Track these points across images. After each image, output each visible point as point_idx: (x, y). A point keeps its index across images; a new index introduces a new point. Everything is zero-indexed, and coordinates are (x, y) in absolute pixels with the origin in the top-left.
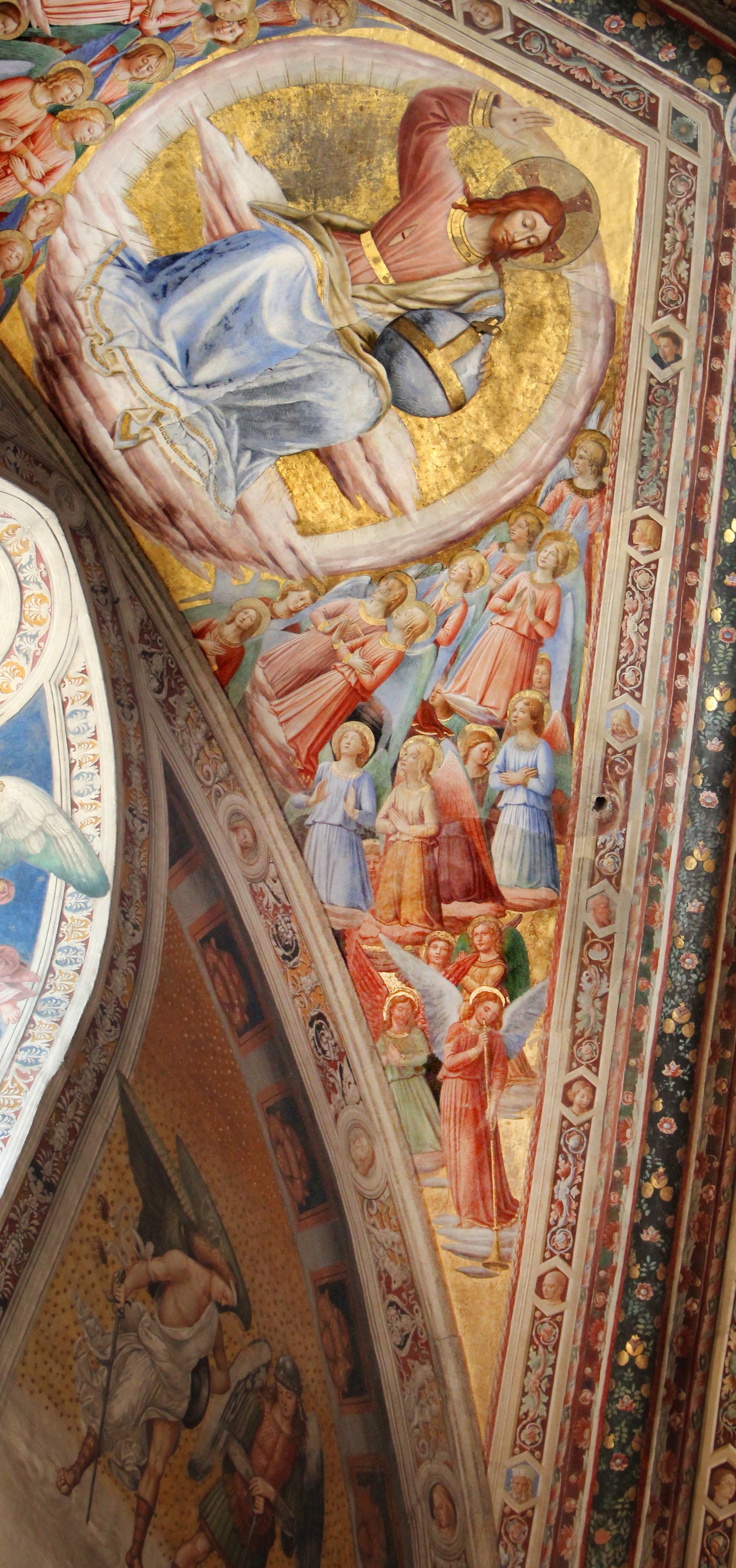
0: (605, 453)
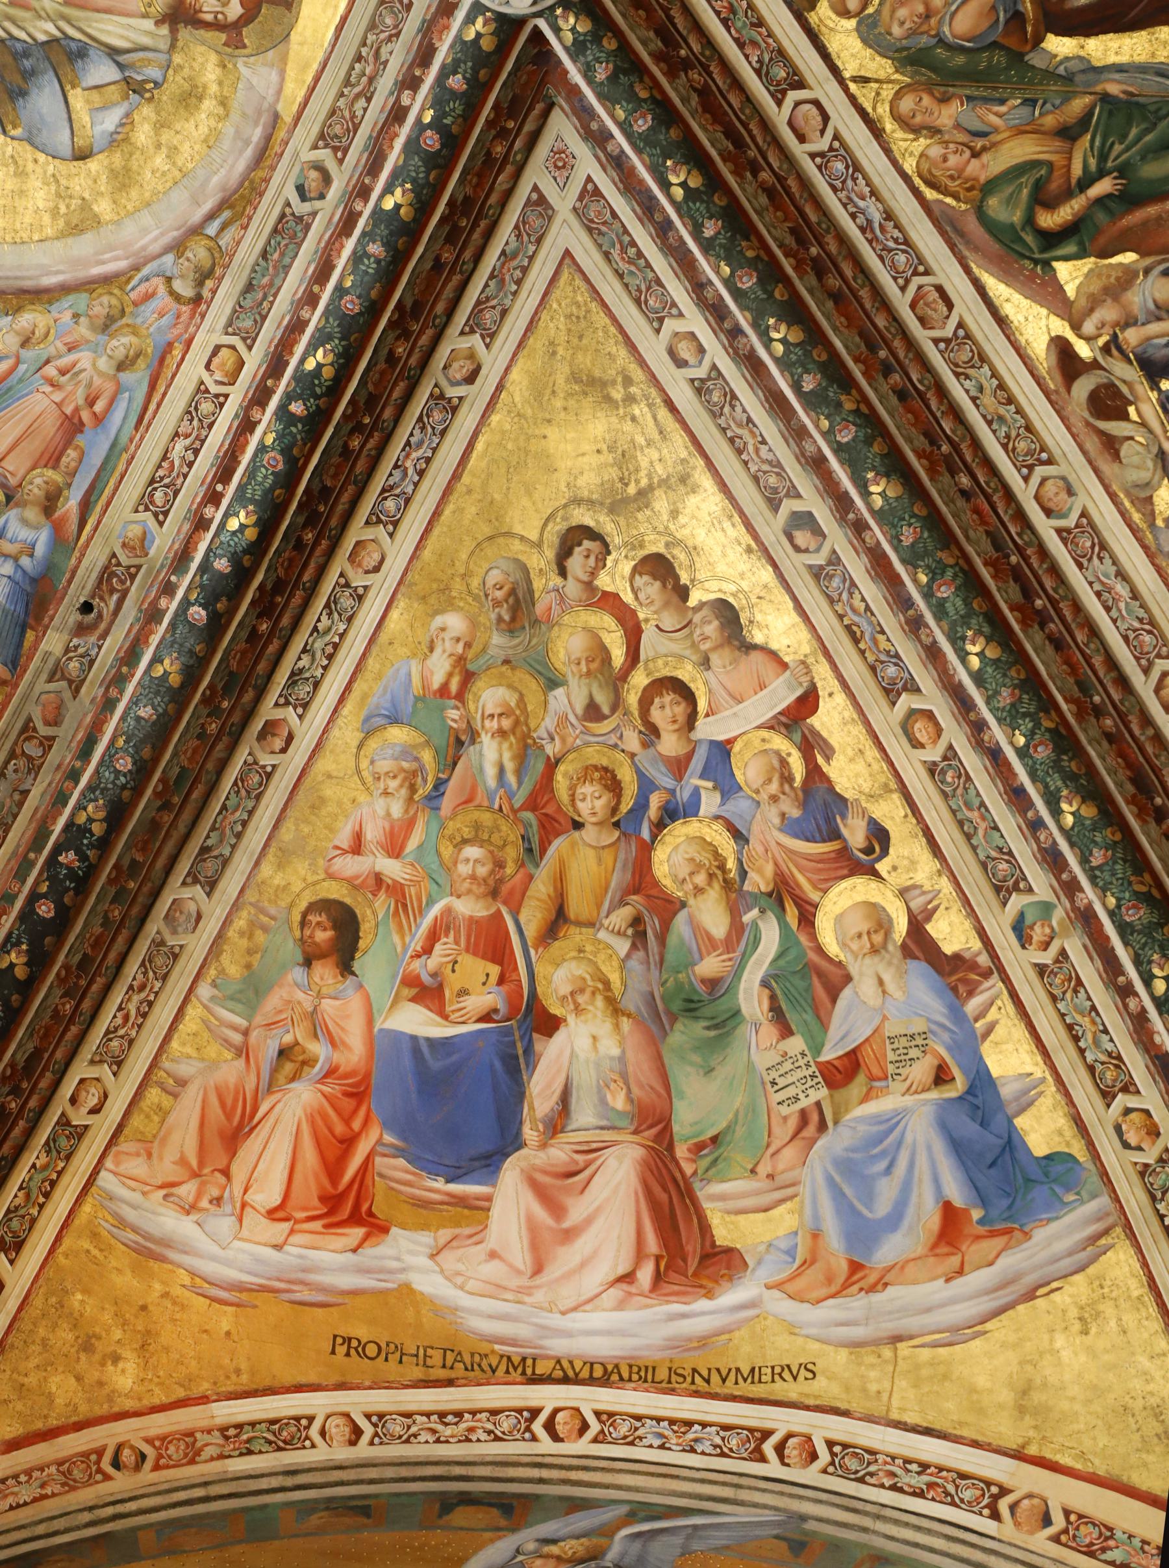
0: (214, 265)
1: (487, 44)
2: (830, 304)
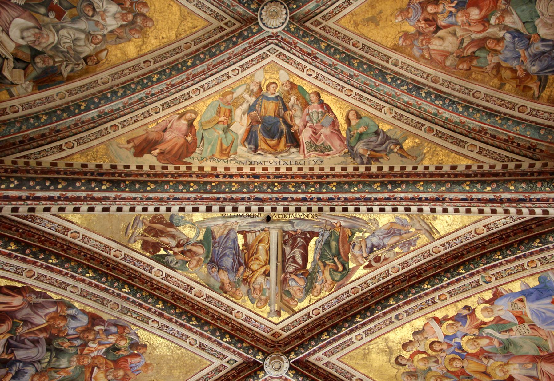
1: (294, 372)
2: (353, 309)
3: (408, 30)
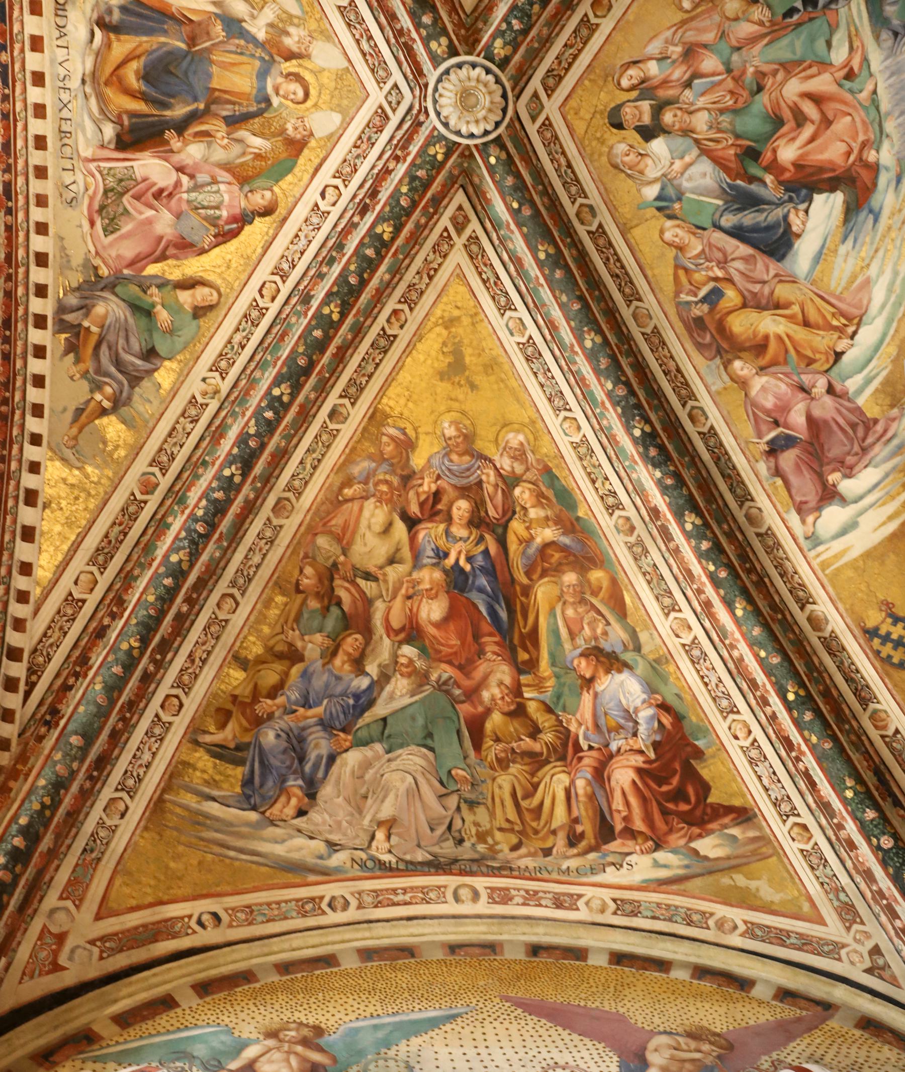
3: (418, 450)
